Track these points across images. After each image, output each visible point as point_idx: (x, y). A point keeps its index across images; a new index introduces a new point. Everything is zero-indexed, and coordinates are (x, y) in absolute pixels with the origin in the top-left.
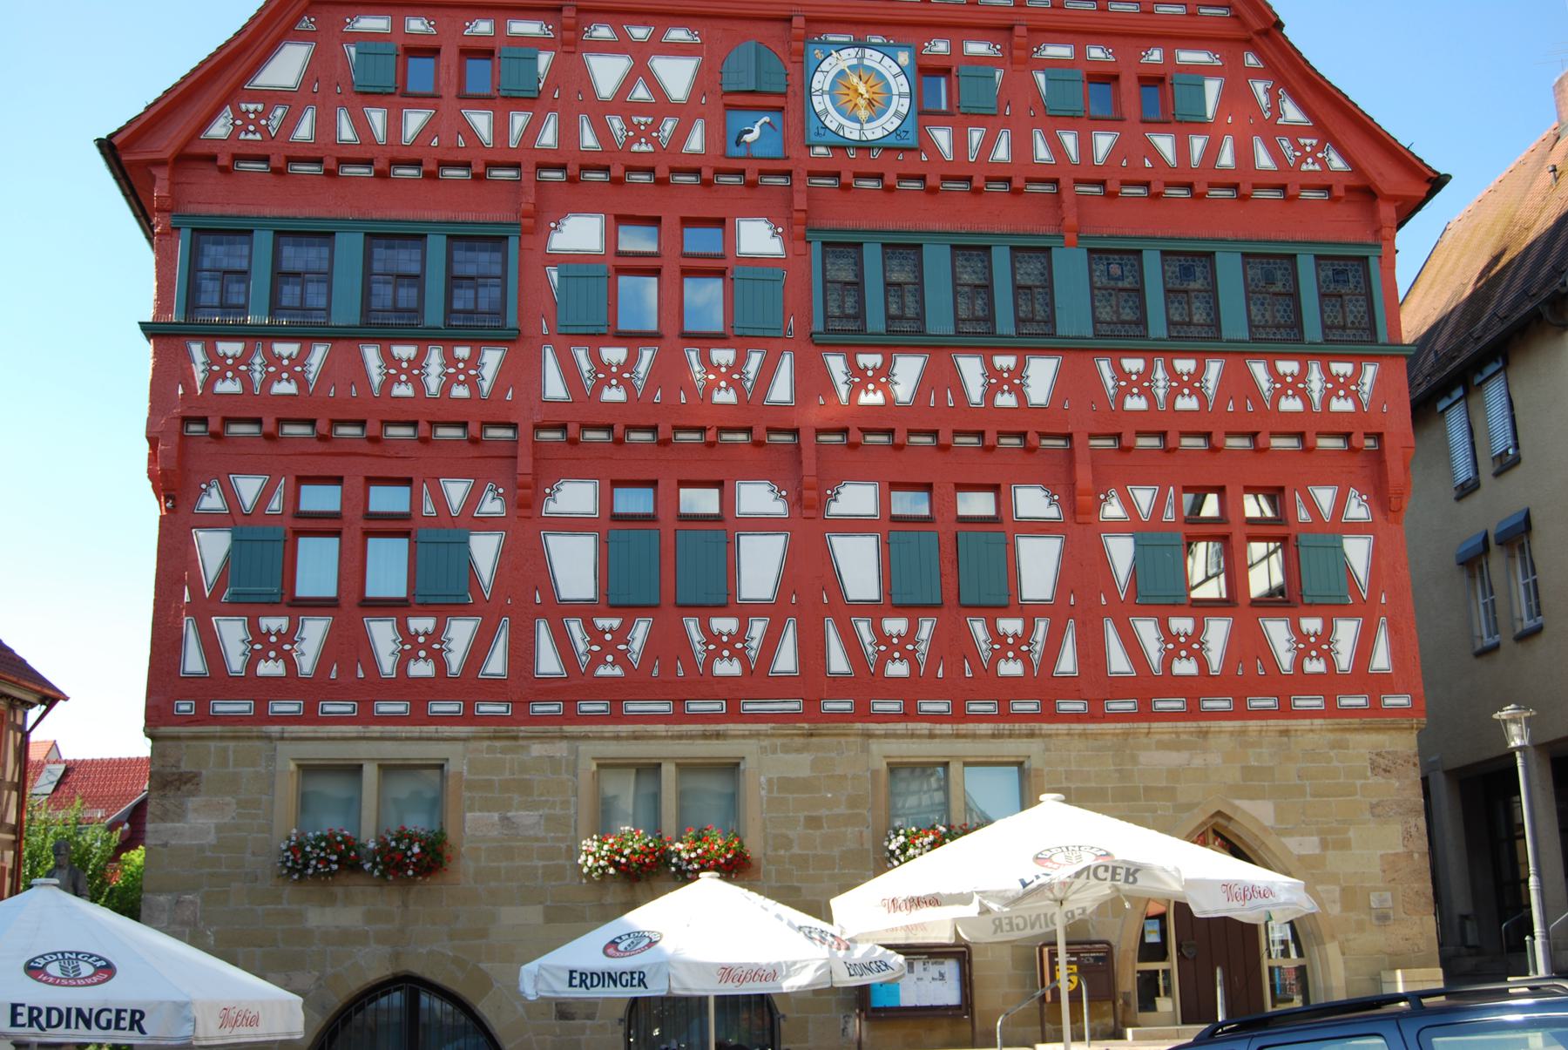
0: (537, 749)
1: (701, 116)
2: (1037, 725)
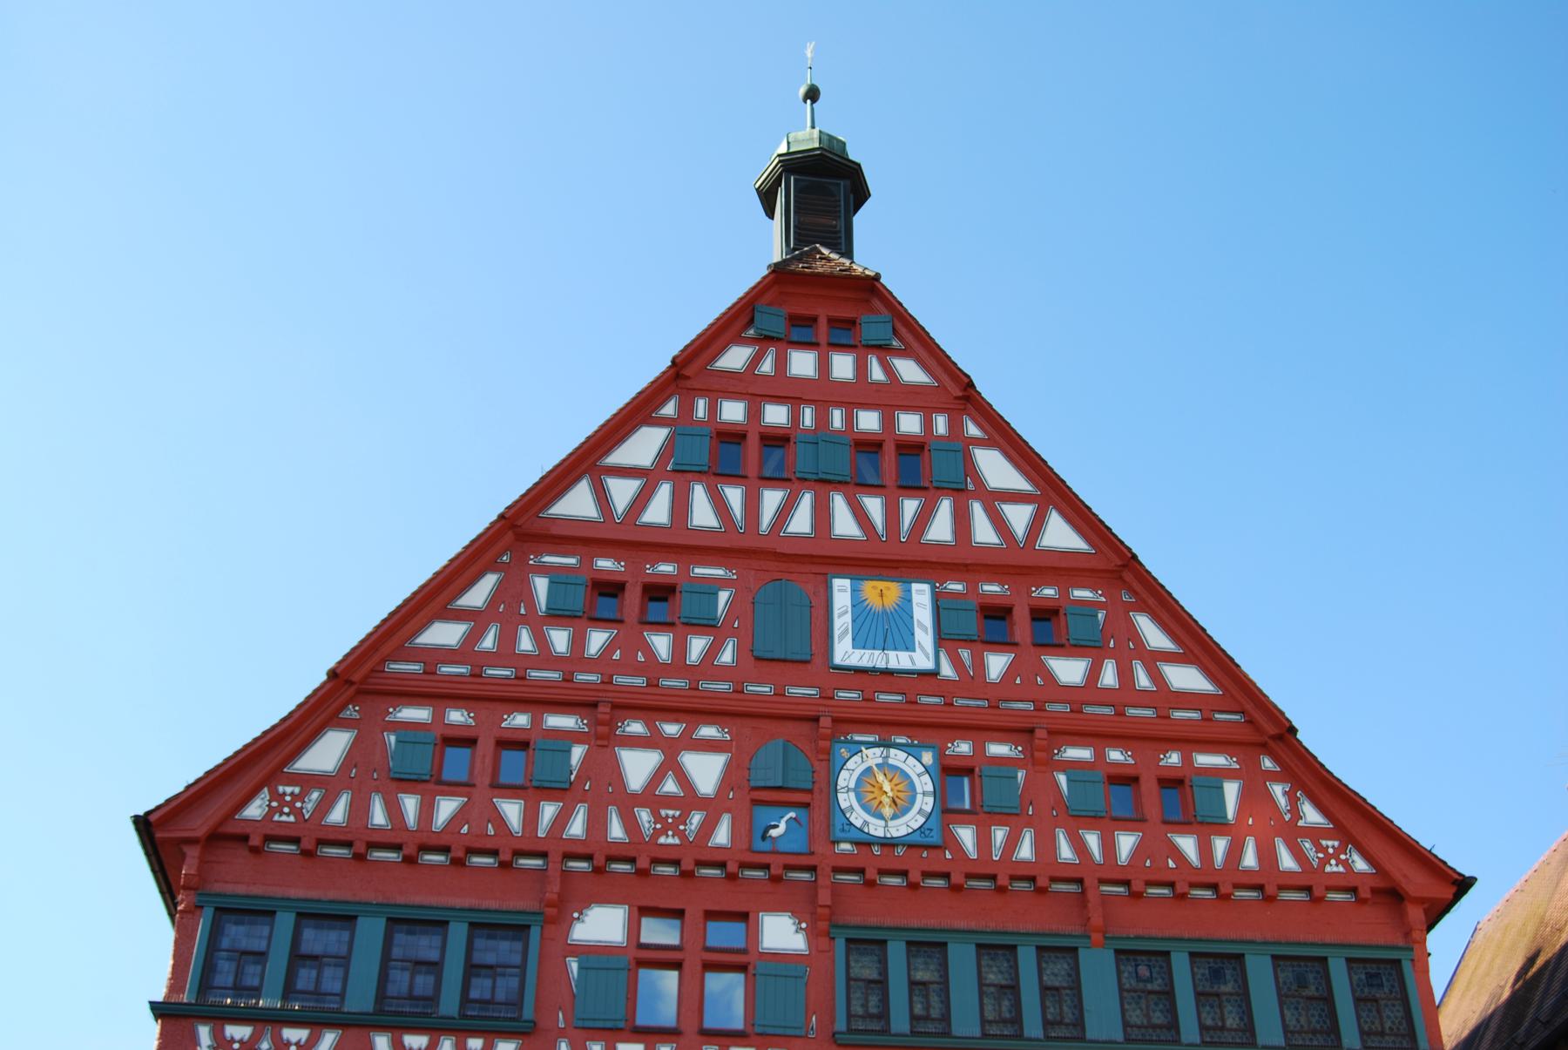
1: (728, 811)
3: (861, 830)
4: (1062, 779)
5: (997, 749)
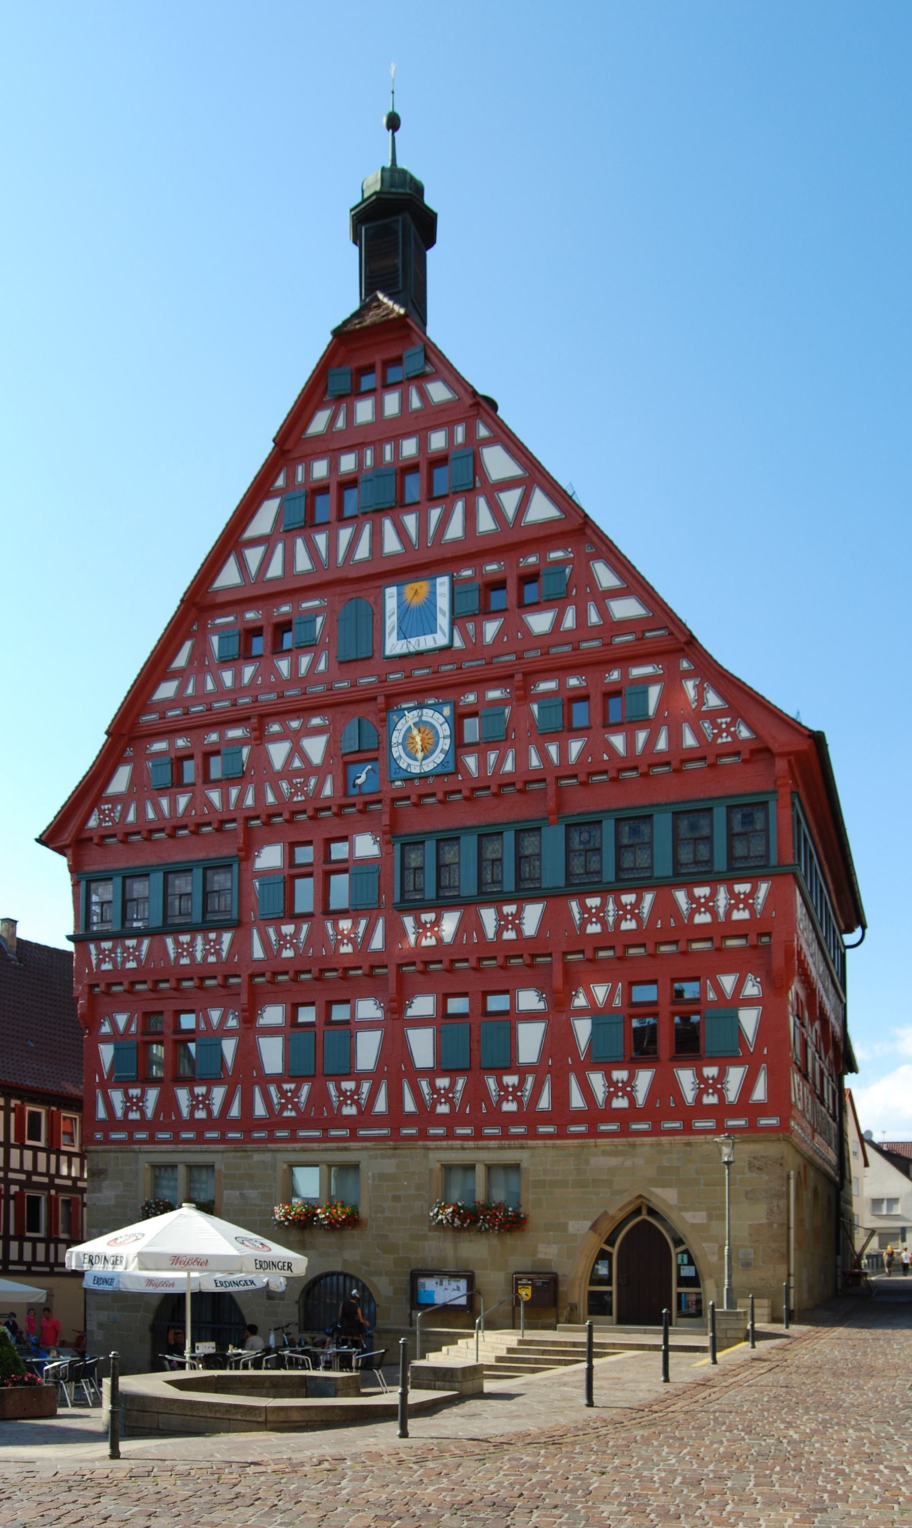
1: (330, 773)
2: (524, 1142)
3: (406, 771)
4: (535, 707)
5: (494, 694)
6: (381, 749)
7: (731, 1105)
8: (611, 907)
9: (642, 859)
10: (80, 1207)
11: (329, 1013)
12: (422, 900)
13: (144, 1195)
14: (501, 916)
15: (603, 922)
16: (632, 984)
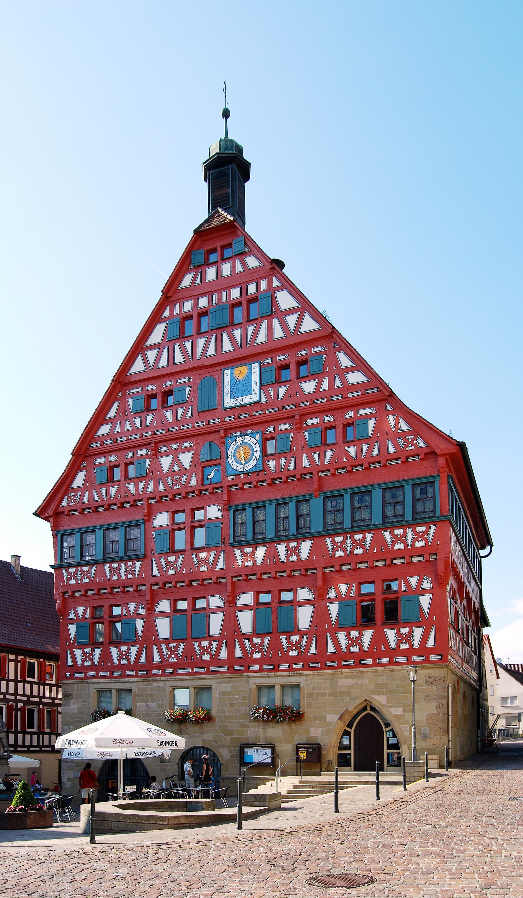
0: (155, 684)
5: (283, 427)
6: (222, 458)
7: (416, 649)
8: (349, 541)
9: (366, 514)
10: (56, 714)
11: (194, 604)
12: (245, 541)
13: (93, 706)
14: (288, 548)
15: (344, 550)
16: (361, 583)
